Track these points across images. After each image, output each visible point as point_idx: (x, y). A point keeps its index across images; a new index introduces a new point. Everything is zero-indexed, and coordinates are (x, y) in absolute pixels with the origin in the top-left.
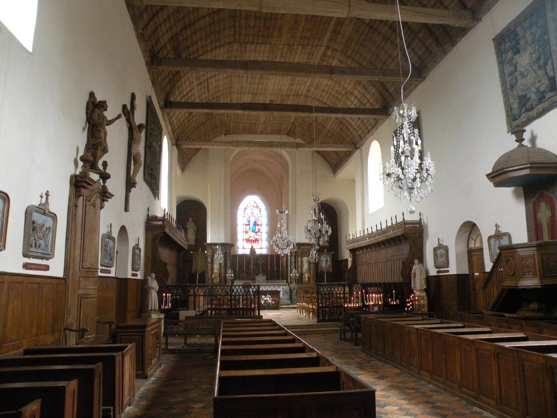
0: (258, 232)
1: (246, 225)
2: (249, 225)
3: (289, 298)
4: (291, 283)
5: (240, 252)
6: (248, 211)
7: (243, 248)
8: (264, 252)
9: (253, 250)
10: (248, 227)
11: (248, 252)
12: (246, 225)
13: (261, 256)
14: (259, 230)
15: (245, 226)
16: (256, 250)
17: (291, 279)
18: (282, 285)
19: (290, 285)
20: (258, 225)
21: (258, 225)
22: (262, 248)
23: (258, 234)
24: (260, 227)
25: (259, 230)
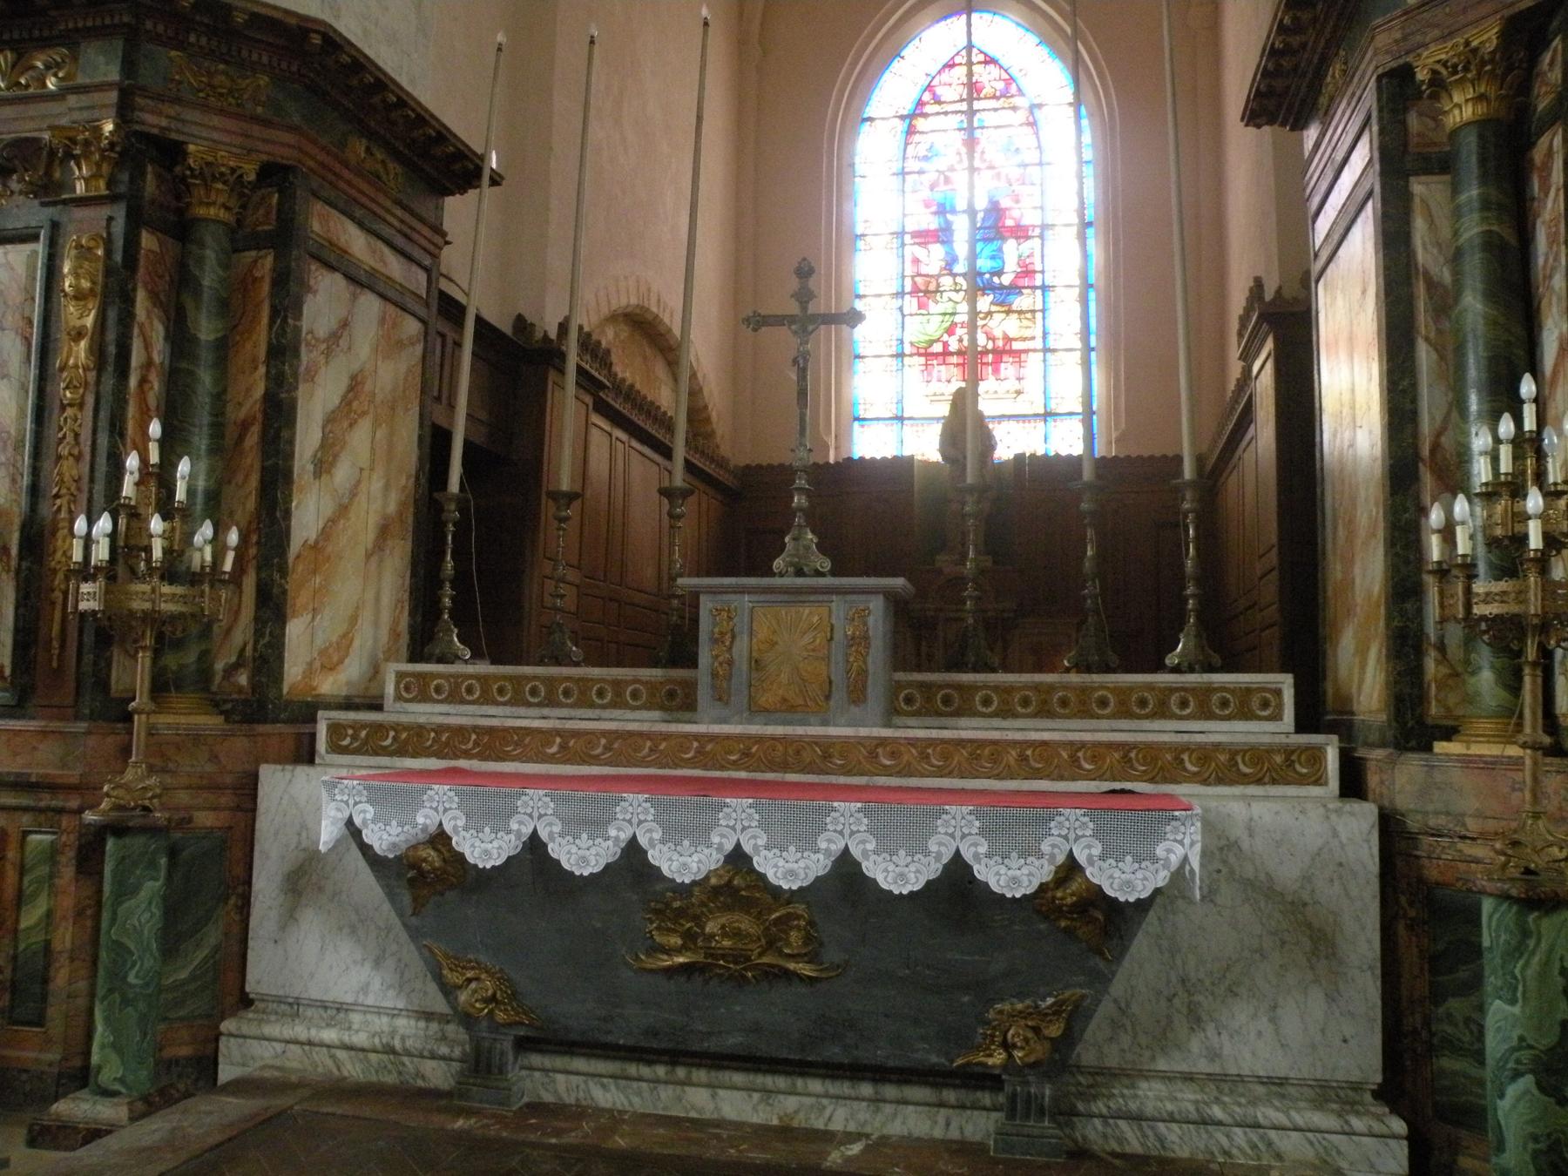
0: (1015, 289)
1: (925, 237)
2: (941, 235)
3: (1363, 1058)
4: (1415, 729)
5: (870, 444)
6: (942, 131)
7: (888, 413)
8: (1067, 441)
9: (965, 427)
10: (933, 258)
11: (925, 446)
12: (925, 237)
13: (1041, 475)
14: (1027, 272)
15: (912, 250)
16: (999, 431)
17: (1406, 644)
18: (1223, 767)
19: (1402, 779)
20: (1021, 233)
21: (1021, 233)
22: (1049, 411)
23: (1022, 302)
24: (1026, 247)
25: (1027, 272)
